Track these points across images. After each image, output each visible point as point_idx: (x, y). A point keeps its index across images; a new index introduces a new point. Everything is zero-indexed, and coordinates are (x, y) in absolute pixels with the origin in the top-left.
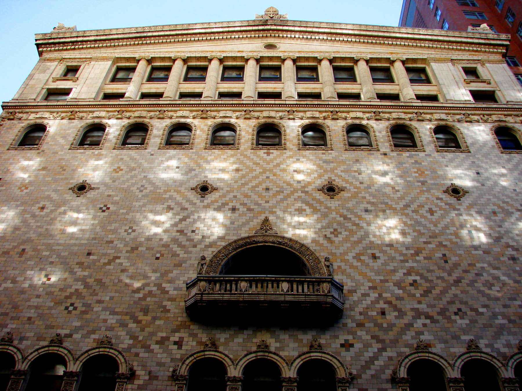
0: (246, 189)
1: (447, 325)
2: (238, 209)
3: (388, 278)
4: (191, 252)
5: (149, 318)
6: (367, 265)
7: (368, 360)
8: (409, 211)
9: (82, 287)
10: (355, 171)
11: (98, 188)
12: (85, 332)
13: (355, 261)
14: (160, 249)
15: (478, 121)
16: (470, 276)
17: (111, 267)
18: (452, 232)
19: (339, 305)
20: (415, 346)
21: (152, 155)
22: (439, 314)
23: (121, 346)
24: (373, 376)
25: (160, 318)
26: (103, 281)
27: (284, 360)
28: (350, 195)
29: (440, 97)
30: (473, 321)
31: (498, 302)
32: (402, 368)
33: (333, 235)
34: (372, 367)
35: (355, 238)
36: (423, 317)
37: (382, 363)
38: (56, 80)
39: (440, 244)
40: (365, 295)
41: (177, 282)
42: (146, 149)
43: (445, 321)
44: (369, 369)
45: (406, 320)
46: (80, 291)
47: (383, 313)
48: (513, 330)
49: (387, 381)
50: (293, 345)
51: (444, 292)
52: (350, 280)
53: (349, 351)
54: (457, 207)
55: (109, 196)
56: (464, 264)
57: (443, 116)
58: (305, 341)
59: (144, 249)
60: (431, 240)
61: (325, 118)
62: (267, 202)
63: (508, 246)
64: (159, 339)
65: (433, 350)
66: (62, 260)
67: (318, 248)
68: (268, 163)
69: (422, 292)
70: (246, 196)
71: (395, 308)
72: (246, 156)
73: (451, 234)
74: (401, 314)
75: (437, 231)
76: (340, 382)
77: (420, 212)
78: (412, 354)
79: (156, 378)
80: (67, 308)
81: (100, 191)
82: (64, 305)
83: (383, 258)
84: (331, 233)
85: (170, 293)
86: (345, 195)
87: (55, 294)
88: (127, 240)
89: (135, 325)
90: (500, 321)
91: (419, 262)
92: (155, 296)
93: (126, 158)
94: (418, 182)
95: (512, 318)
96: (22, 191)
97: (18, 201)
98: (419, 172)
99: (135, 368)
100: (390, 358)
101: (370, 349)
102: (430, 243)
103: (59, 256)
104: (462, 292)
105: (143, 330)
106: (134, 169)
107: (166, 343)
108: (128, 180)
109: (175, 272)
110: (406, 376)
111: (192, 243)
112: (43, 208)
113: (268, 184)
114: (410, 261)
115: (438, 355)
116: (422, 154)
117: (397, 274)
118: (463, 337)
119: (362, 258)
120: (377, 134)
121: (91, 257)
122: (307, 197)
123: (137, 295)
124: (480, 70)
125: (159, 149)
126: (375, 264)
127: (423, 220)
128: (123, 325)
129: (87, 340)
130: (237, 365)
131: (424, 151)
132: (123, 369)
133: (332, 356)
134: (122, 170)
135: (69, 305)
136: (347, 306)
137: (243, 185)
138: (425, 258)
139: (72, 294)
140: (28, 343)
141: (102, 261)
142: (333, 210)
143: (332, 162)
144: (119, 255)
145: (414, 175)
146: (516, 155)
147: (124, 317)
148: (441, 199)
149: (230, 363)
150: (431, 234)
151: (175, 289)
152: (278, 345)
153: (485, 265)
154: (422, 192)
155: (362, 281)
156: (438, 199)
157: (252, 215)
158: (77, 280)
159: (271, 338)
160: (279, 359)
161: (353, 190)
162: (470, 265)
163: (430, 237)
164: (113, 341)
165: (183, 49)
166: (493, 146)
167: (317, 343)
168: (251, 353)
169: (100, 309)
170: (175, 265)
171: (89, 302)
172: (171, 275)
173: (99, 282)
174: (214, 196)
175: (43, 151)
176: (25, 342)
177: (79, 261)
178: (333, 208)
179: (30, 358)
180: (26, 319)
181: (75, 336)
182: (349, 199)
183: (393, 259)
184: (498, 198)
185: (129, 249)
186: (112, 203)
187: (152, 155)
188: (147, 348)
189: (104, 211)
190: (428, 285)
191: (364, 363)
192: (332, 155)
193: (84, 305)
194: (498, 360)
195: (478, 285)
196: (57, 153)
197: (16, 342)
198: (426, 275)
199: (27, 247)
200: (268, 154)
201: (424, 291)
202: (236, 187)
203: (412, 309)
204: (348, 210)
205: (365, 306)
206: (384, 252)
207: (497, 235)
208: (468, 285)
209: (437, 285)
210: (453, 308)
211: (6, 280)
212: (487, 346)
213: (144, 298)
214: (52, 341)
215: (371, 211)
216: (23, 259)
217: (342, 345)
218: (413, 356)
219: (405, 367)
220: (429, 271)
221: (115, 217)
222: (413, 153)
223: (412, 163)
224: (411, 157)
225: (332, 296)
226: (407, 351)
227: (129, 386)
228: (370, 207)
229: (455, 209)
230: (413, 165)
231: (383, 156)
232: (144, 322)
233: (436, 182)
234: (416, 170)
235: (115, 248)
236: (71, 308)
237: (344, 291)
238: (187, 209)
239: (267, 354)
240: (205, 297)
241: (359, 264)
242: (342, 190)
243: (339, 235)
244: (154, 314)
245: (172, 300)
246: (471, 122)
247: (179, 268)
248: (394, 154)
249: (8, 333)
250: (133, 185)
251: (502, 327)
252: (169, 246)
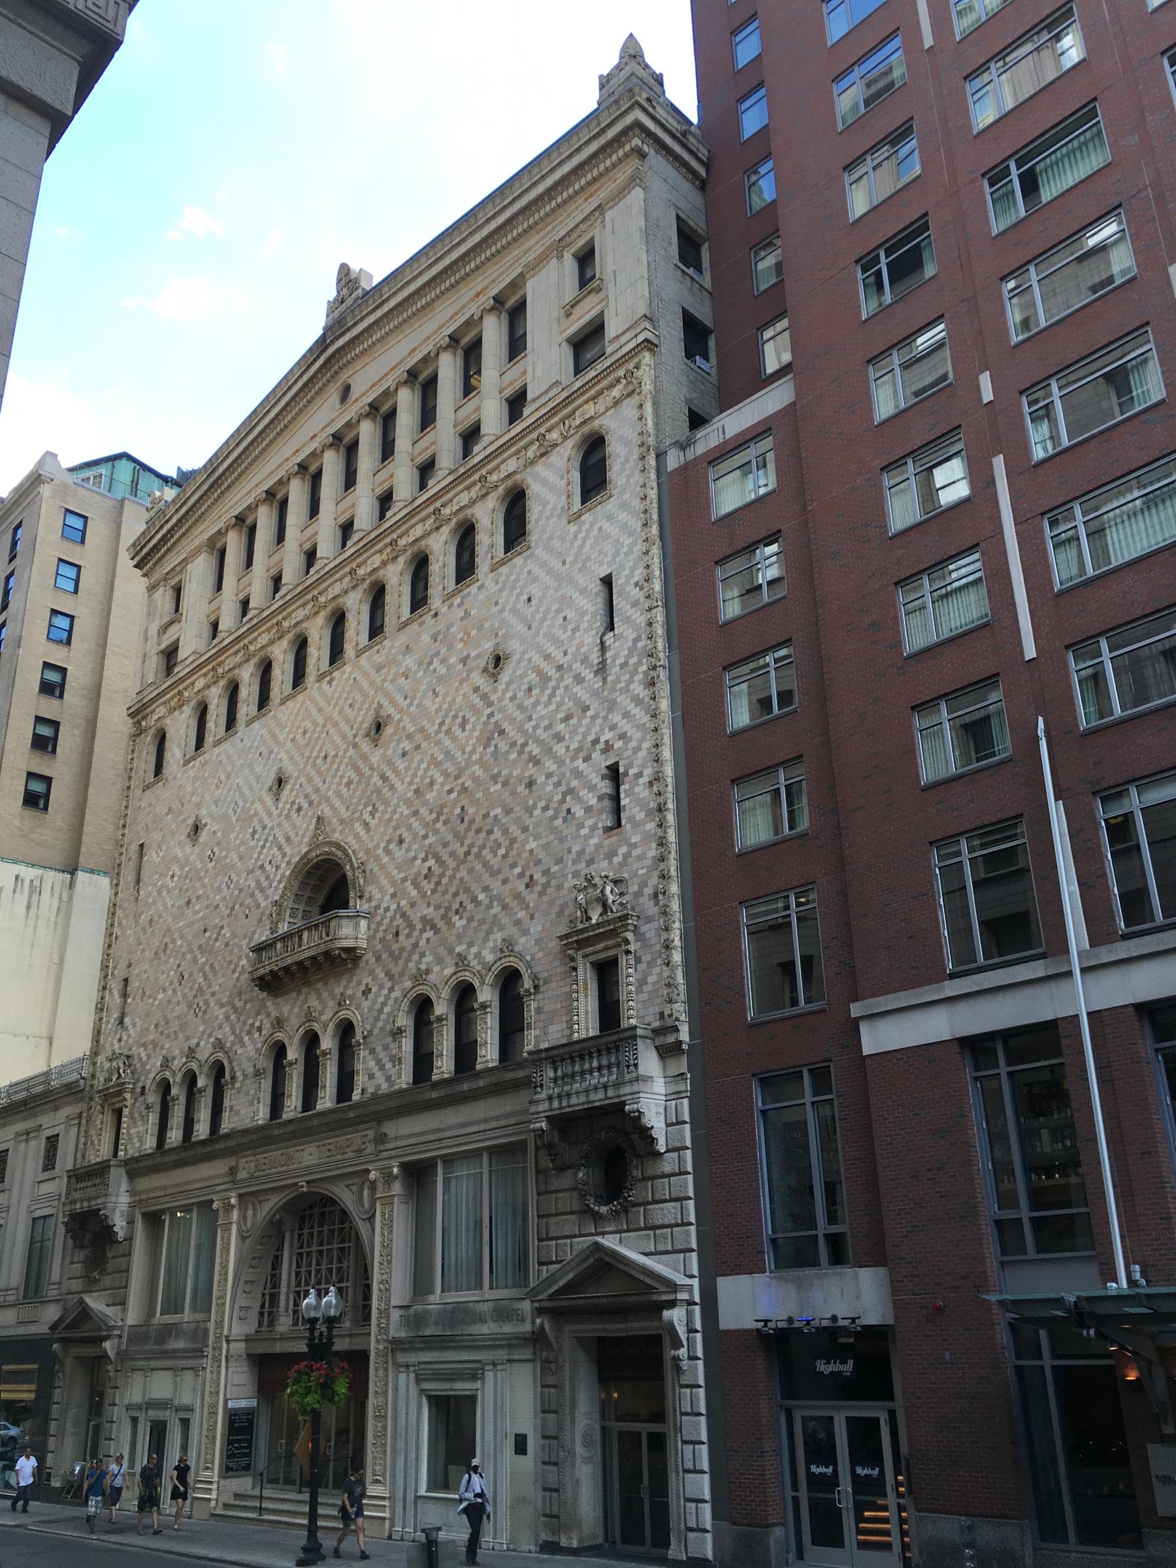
40: (387, 909)
47: (397, 934)
100: (396, 1000)
210: (456, 906)
251: (495, 921)
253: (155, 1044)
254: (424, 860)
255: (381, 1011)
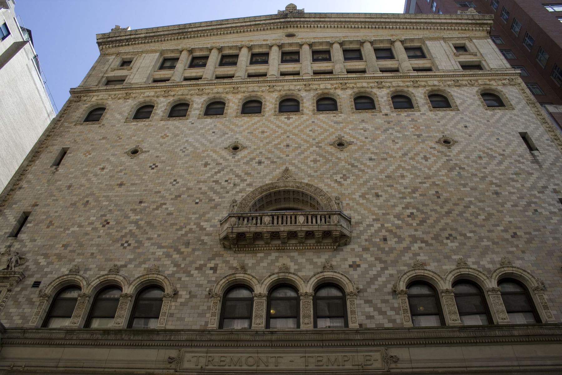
0: (269, 147)
1: (440, 248)
2: (264, 162)
3: (389, 211)
4: (224, 197)
5: (189, 250)
6: (371, 202)
7: (373, 277)
8: (406, 158)
9: (135, 228)
10: (361, 129)
11: (149, 151)
12: (137, 263)
13: (361, 198)
14: (198, 196)
15: (466, 85)
16: (460, 208)
17: (159, 211)
18: (444, 174)
19: (347, 233)
20: (412, 265)
21: (193, 123)
22: (432, 239)
23: (167, 273)
24: (376, 290)
25: (198, 250)
26: (152, 222)
27: (302, 279)
28: (357, 148)
29: (433, 68)
30: (462, 244)
31: (484, 228)
32: (401, 283)
33: (342, 180)
34: (376, 282)
35: (361, 181)
36: (419, 242)
37: (384, 279)
38: (113, 70)
39: (434, 184)
40: (370, 226)
41: (213, 221)
42: (187, 119)
43: (439, 244)
44: (374, 284)
45: (405, 244)
46: (133, 231)
47: (385, 239)
48: (496, 250)
49: (389, 294)
50: (309, 267)
51: (437, 221)
52: (356, 214)
53: (356, 270)
54: (448, 154)
55: (157, 157)
56: (454, 199)
57: (436, 83)
58: (319, 264)
59: (185, 196)
60: (426, 180)
61: (335, 89)
62: (288, 156)
63: (492, 183)
64: (198, 266)
65: (428, 268)
66: (118, 208)
67: (330, 190)
68: (288, 126)
69: (418, 222)
70: (270, 152)
71: (395, 235)
72: (270, 121)
73: (443, 175)
74: (400, 239)
75: (431, 174)
76: (348, 295)
77: (416, 158)
78: (410, 271)
79: (195, 296)
80: (122, 245)
81: (150, 153)
82: (120, 242)
83: (385, 196)
84: (341, 178)
85: (207, 229)
86: (353, 147)
87: (113, 234)
88: (172, 190)
89: (178, 256)
90: (485, 243)
91: (416, 198)
92: (194, 232)
93: (171, 127)
94: (414, 135)
95: (496, 240)
96: (86, 156)
97: (82, 164)
98: (416, 128)
99: (178, 289)
100: (391, 275)
101: (374, 268)
102: (425, 183)
103: (116, 205)
104: (452, 221)
105: (184, 259)
106: (177, 135)
107: (204, 269)
108: (173, 144)
109: (211, 213)
110: (405, 289)
111: (225, 190)
112: (103, 169)
113: (288, 142)
114: (408, 198)
115: (432, 272)
116: (418, 114)
117: (397, 208)
118: (454, 257)
119: (367, 196)
120: (380, 99)
121: (143, 205)
122: (321, 151)
123: (180, 233)
124: (468, 45)
125: (198, 119)
126: (378, 201)
127: (419, 165)
128: (168, 256)
129: (139, 269)
130: (262, 283)
131: (420, 111)
132: (168, 290)
133: (342, 274)
134: (168, 136)
135: (124, 242)
136: (354, 234)
137: (268, 143)
138: (420, 195)
139: (126, 234)
140: (92, 273)
141: (152, 207)
142: (342, 160)
143: (342, 123)
144: (165, 202)
145: (411, 130)
146: (499, 111)
147: (169, 250)
148: (434, 148)
149: (257, 282)
150: (425, 176)
151: (211, 226)
152: (296, 267)
153: (473, 199)
154: (418, 143)
155: (366, 215)
156: (431, 148)
157: (275, 166)
158: (131, 223)
159: (291, 261)
160: (298, 278)
161: (359, 144)
162: (459, 199)
163: (425, 178)
164: (161, 269)
165: (218, 41)
166: (479, 105)
167: (329, 265)
168: (274, 274)
169: (150, 244)
170: (211, 208)
171: (140, 239)
172: (207, 216)
173: (149, 223)
174: (243, 153)
175: (103, 125)
176: (88, 272)
177: (132, 208)
178: (342, 158)
179: (92, 284)
180: (90, 254)
181: (129, 266)
182: (356, 151)
183: (393, 196)
184: (484, 146)
185: (174, 197)
186: (160, 162)
187: (193, 123)
188: (189, 274)
189: (153, 169)
190: (423, 216)
191: (369, 280)
192: (340, 117)
193: (136, 242)
194: (484, 274)
195: (467, 215)
196: (115, 126)
197: (81, 273)
198: (421, 207)
199: (90, 199)
200: (288, 119)
201: (420, 221)
202: (262, 145)
203: (410, 236)
204: (355, 159)
205: (370, 234)
206: (386, 192)
207: (482, 175)
208: (457, 215)
209: (431, 216)
210: (446, 234)
211: (73, 225)
212: (474, 263)
213: (186, 234)
214: (110, 271)
215: (374, 159)
216: (87, 208)
217: (350, 266)
218: (411, 273)
219: (404, 282)
220: (424, 205)
221: (162, 172)
222: (410, 113)
223: (410, 121)
224: (408, 116)
225: (341, 225)
226: (405, 268)
227: (173, 304)
228: (373, 156)
229: (446, 156)
230: (411, 123)
231: (385, 116)
232: (185, 253)
233: (430, 135)
234: (412, 126)
235: (163, 197)
236: (126, 245)
237: (352, 223)
238: (221, 164)
239: (287, 274)
240: (235, 230)
241: (364, 201)
242: (350, 143)
243: (348, 180)
244: (194, 247)
245: (208, 234)
246: (459, 86)
247: (215, 210)
248: (394, 114)
249: (75, 266)
250: (177, 147)
251: (487, 248)
252: (206, 193)
253: (60, 257)
254: (406, 207)
255: (375, 277)
